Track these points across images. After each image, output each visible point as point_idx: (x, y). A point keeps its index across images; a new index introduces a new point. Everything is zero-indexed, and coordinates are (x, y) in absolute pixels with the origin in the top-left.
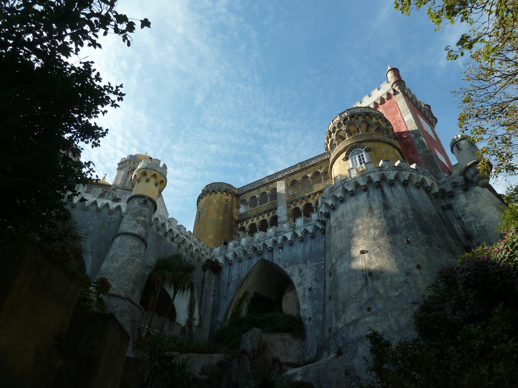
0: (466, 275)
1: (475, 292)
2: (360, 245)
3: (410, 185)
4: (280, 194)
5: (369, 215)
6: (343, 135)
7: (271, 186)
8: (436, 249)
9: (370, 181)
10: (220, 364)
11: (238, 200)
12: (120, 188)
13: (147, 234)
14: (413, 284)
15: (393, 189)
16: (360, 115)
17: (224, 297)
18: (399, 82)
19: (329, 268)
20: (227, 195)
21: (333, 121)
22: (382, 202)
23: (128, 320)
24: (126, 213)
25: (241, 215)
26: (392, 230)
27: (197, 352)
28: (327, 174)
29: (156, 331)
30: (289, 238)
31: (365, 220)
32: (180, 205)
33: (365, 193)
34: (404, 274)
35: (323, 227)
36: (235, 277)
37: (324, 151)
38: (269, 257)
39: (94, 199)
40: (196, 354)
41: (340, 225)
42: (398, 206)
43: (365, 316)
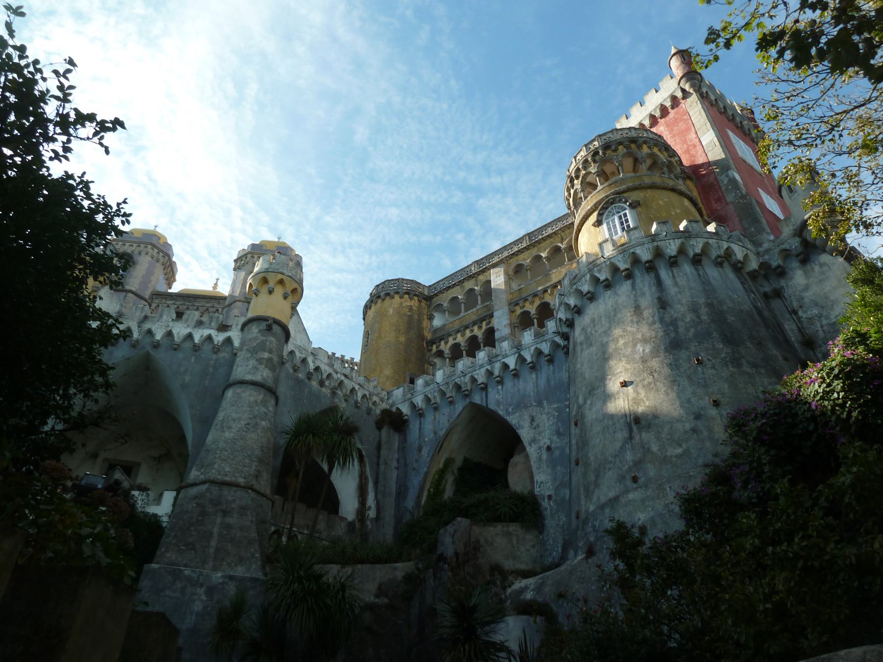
0: (759, 424)
1: (772, 452)
2: (620, 371)
3: (705, 261)
4: (496, 290)
5: (635, 320)
6: (593, 182)
7: (482, 278)
8: (748, 370)
9: (636, 260)
10: (409, 578)
11: (429, 306)
12: (240, 301)
13: (276, 380)
14: (705, 433)
15: (675, 270)
16: (620, 143)
17: (414, 469)
18: (691, 75)
19: (574, 413)
20: (411, 299)
21: (575, 158)
22: (656, 296)
23: (252, 521)
24: (241, 349)
25: (436, 331)
26: (673, 344)
27: (371, 562)
28: (572, 249)
29: (305, 532)
30: (512, 366)
31: (629, 329)
32: (331, 322)
33: (629, 282)
34: (692, 417)
35: (566, 343)
36: (429, 436)
37: (567, 211)
38: (482, 399)
39: (188, 330)
40: (368, 566)
41: (588, 341)
42: (684, 301)
43: (627, 491)
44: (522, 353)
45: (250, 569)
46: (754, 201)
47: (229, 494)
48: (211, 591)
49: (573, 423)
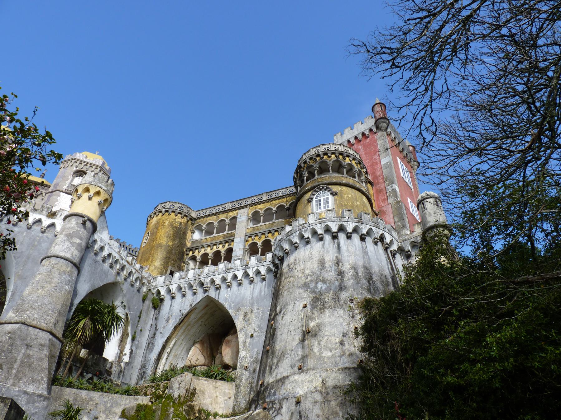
3: (368, 239)
7: (232, 214)
16: (333, 153)
17: (161, 333)
20: (183, 218)
22: (336, 255)
25: (194, 242)
34: (342, 335)
35: (276, 270)
43: (295, 374)
44: (247, 270)
46: (404, 206)
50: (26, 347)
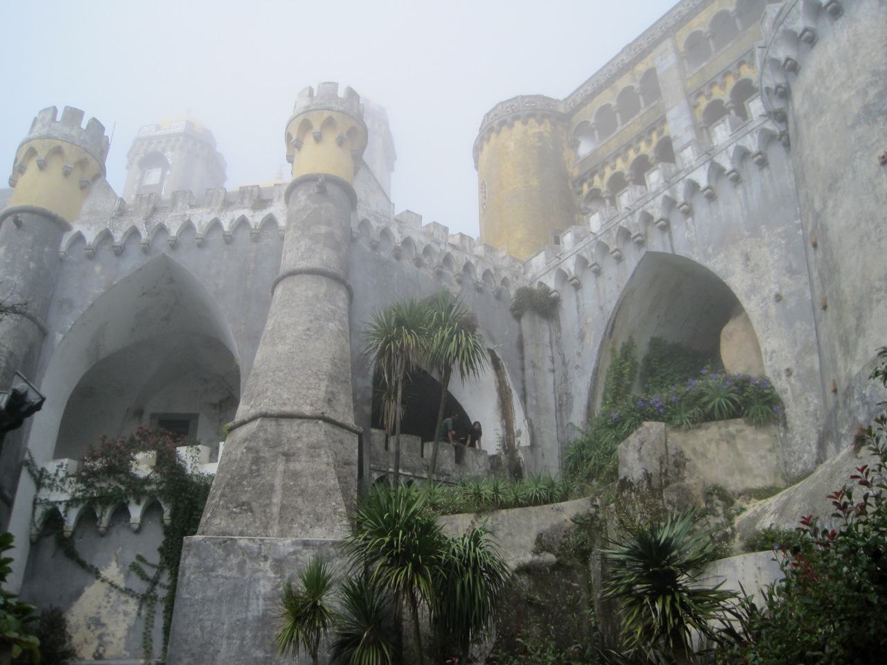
7: (641, 68)
17: (577, 367)
20: (540, 122)
23: (328, 464)
24: (288, 228)
27: (521, 505)
30: (703, 181)
35: (783, 129)
39: (213, 216)
40: (517, 510)
44: (716, 159)
45: (336, 530)
47: (290, 430)
48: (279, 565)
49: (810, 246)
50: (284, 458)
